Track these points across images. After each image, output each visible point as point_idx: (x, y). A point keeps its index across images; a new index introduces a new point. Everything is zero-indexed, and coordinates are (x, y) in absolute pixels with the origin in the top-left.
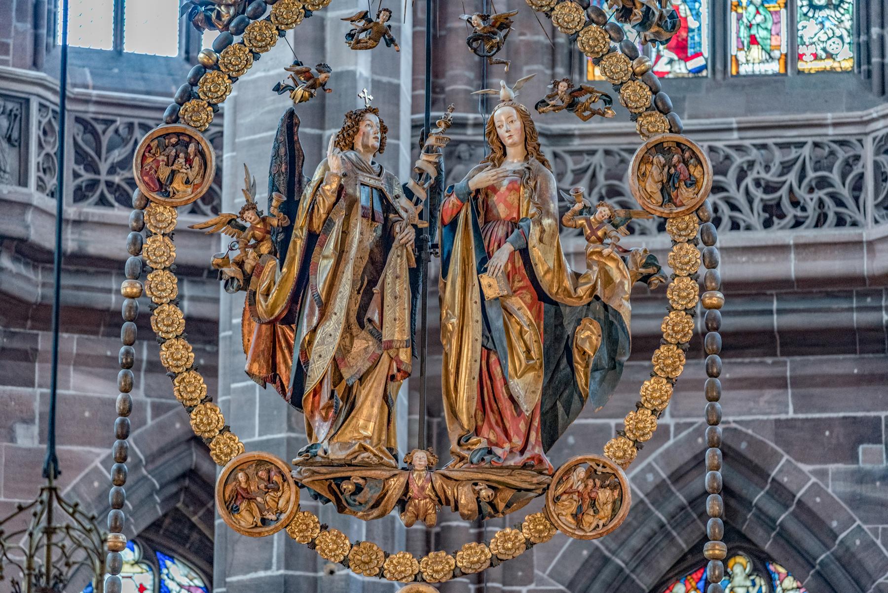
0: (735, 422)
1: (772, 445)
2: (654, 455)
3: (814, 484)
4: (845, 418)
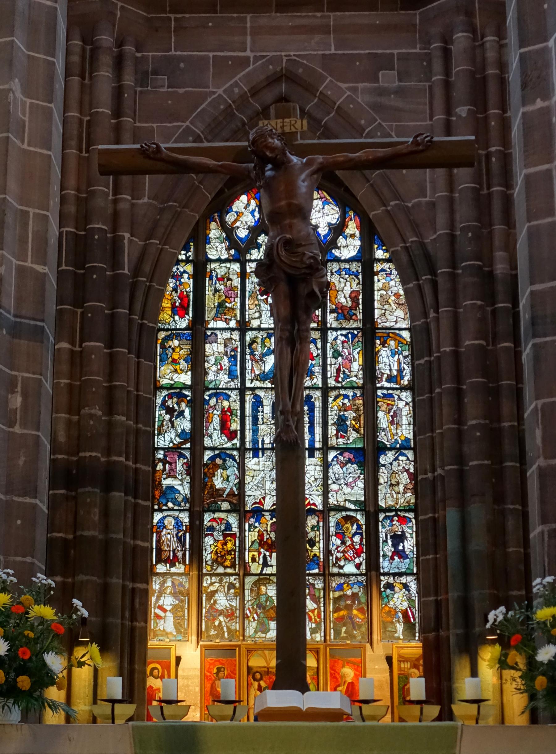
0: (294, 55)
1: (321, 70)
2: (239, 76)
3: (348, 96)
4: (369, 53)
